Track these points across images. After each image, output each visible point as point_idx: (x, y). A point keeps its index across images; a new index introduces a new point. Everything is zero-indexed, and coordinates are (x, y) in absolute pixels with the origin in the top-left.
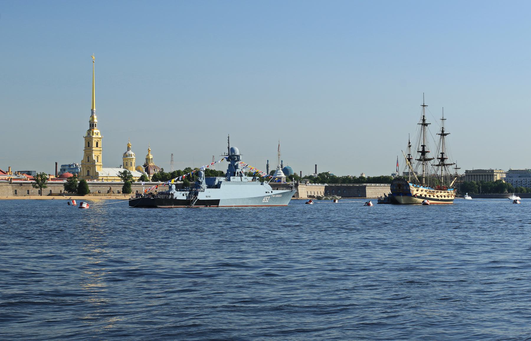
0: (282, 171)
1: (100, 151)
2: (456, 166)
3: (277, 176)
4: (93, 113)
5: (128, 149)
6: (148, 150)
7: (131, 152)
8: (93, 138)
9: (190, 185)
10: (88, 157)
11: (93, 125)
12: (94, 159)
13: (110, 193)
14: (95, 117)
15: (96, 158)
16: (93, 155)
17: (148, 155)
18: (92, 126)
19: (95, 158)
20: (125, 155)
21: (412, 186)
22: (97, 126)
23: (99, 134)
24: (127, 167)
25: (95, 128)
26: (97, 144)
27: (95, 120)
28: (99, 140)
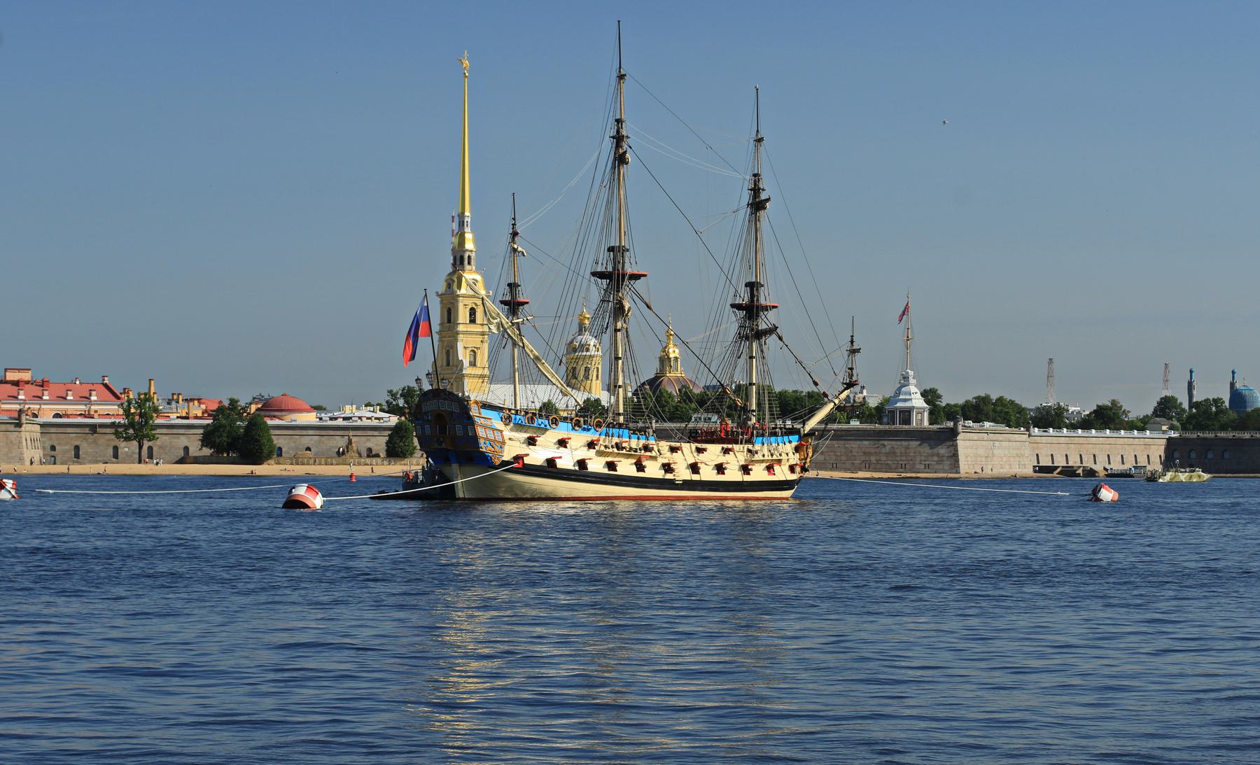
0: (917, 390)
1: (483, 335)
2: (852, 342)
3: (899, 405)
4: (462, 224)
8: (458, 296)
10: (448, 353)
11: (462, 258)
13: (348, 455)
15: (468, 356)
16: (460, 346)
17: (666, 347)
19: (463, 355)
21: (499, 425)
22: (472, 262)
25: (467, 267)
26: (473, 312)
27: (469, 245)
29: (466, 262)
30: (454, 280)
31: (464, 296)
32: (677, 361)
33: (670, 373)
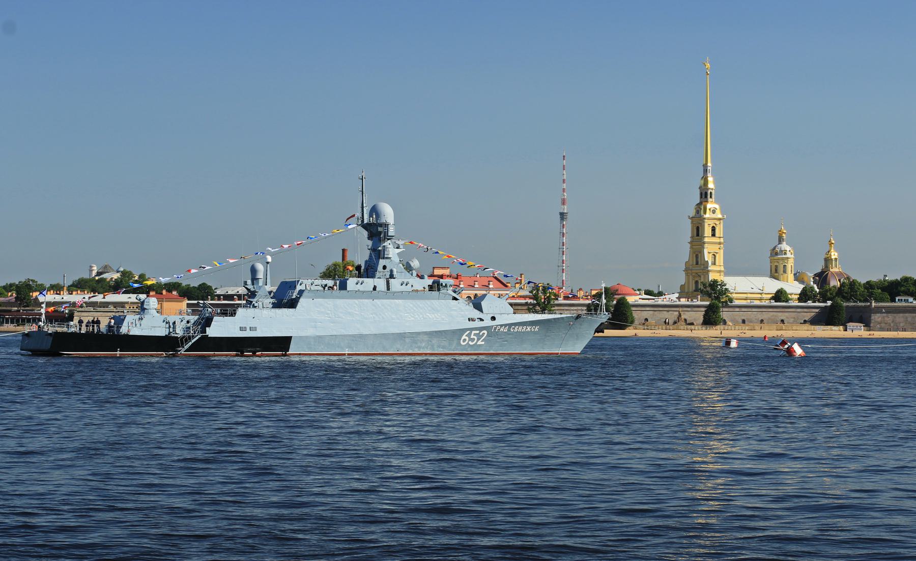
1: (720, 244)
4: (706, 171)
5: (780, 240)
6: (830, 241)
7: (785, 246)
8: (705, 219)
9: (844, 309)
10: (697, 256)
11: (706, 193)
12: (706, 260)
13: (679, 324)
14: (710, 179)
15: (711, 258)
16: (706, 251)
17: (829, 252)
18: (703, 197)
19: (708, 257)
20: (774, 253)
22: (713, 196)
23: (718, 211)
24: (777, 274)
25: (710, 200)
26: (714, 229)
27: (711, 185)
28: (717, 222)
29: (709, 196)
30: (700, 207)
31: (708, 219)
32: (836, 261)
33: (832, 269)
